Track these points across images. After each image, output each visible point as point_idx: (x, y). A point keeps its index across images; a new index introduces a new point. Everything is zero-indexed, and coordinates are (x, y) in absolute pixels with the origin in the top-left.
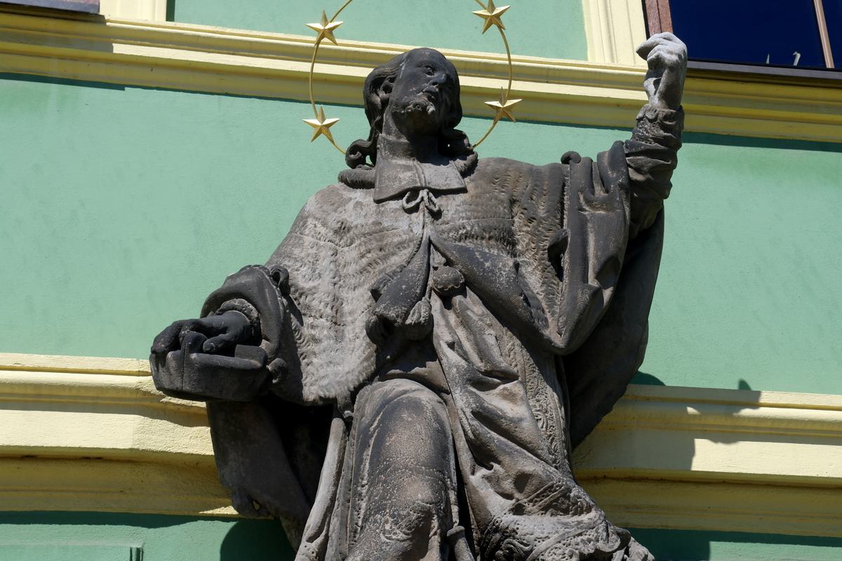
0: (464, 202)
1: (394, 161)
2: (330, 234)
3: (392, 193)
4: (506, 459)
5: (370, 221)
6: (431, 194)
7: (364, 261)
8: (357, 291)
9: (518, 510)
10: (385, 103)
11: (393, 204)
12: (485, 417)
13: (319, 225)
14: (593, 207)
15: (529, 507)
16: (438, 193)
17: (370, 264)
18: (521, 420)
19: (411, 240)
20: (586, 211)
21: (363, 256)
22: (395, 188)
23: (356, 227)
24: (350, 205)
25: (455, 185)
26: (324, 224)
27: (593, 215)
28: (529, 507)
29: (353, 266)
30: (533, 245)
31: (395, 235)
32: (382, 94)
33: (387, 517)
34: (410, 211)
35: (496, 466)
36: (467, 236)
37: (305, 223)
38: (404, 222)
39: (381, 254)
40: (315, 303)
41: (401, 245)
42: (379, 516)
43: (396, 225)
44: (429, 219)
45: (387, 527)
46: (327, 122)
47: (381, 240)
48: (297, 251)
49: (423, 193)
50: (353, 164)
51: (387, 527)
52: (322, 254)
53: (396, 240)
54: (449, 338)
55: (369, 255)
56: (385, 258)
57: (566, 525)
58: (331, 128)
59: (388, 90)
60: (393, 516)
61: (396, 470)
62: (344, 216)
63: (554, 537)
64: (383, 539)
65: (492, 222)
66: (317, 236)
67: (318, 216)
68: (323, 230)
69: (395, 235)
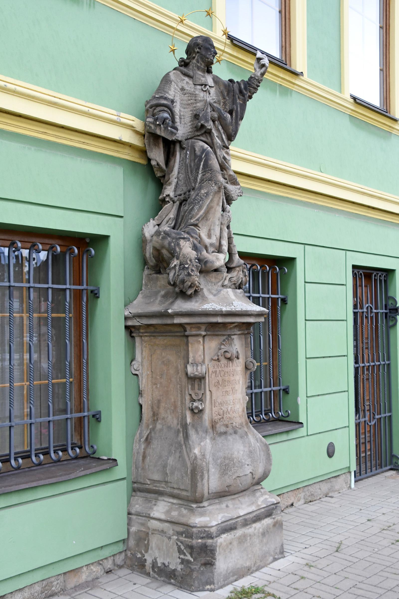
1: (198, 72)
2: (179, 89)
3: (199, 84)
4: (228, 170)
5: (192, 90)
7: (189, 102)
8: (186, 110)
9: (227, 183)
10: (198, 52)
11: (199, 87)
12: (224, 158)
13: (175, 85)
14: (240, 100)
16: (209, 86)
17: (191, 104)
19: (204, 100)
21: (189, 100)
22: (200, 82)
23: (187, 90)
24: (185, 82)
26: (177, 86)
27: (239, 102)
28: (229, 183)
29: (185, 102)
30: (224, 106)
31: (199, 97)
32: (198, 50)
33: (213, 183)
34: (204, 91)
35: (225, 172)
37: (171, 83)
38: (202, 94)
39: (195, 102)
40: (176, 111)
41: (201, 101)
42: (210, 182)
43: (200, 94)
45: (213, 185)
46: (175, 48)
47: (196, 97)
48: (170, 92)
49: (208, 87)
50: (181, 66)
51: (213, 185)
52: (176, 95)
53: (200, 99)
54: (216, 135)
55: (191, 101)
56: (196, 103)
57: (236, 188)
58: (175, 51)
59: (200, 48)
60: (215, 183)
61: (214, 171)
62: (183, 85)
63: (234, 191)
64: (212, 188)
66: (175, 89)
67: (176, 82)
68: (177, 88)
69: (199, 97)
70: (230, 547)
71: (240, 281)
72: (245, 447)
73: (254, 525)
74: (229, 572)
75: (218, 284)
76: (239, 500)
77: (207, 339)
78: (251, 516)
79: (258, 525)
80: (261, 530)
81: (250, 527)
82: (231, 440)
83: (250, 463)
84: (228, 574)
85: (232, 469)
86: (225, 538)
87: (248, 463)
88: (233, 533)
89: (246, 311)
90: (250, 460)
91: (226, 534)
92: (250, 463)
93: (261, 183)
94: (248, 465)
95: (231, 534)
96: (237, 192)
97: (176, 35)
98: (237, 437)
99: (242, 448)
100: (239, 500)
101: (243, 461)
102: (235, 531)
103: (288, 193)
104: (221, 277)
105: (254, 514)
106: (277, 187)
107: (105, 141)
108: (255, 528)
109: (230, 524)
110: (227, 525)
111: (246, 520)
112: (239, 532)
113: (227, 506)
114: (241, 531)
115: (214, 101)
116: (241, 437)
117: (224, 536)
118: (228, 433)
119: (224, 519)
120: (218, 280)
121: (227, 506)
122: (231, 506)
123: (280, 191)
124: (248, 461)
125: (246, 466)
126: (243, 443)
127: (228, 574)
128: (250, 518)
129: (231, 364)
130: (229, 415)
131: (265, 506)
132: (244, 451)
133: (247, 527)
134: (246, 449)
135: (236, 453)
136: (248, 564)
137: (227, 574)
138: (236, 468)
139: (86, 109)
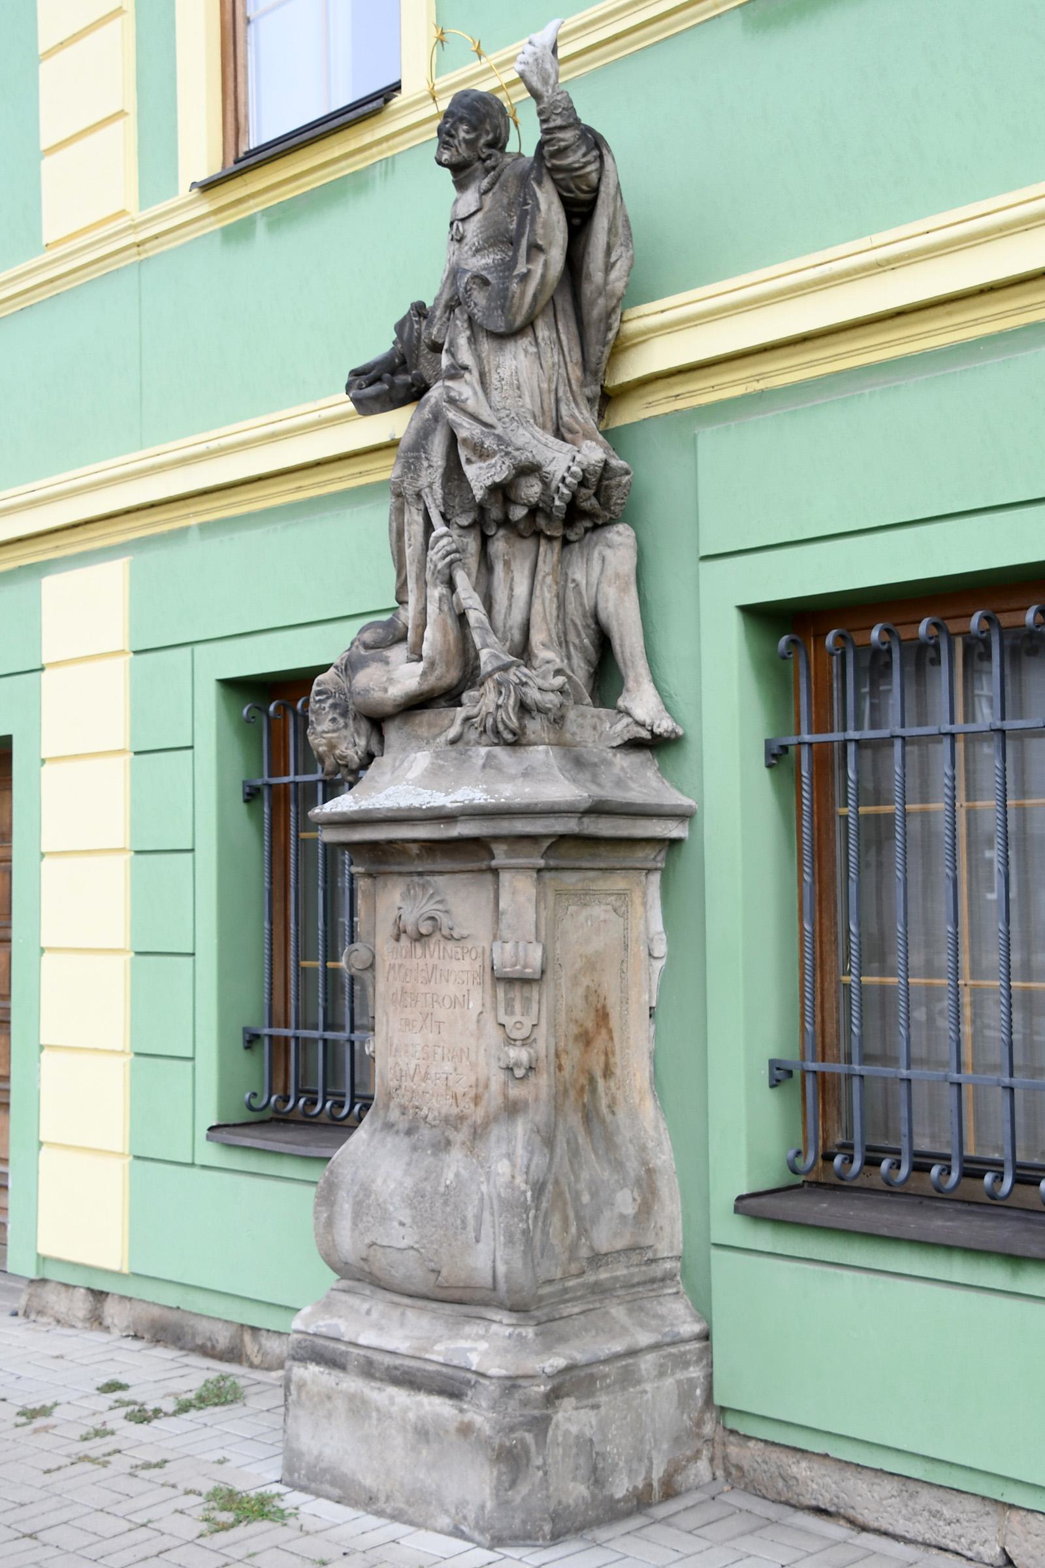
0: (479, 221)
6: (460, 224)
15: (474, 459)
16: (463, 220)
18: (467, 399)
20: (528, 204)
25: (473, 209)
28: (474, 459)
36: (477, 251)
44: (457, 246)
57: (480, 468)
65: (490, 232)
70: (328, 1405)
71: (490, 721)
72: (406, 1173)
73: (392, 1390)
74: (323, 1465)
75: (438, 740)
76: (403, 1314)
77: (380, 881)
78: (388, 1360)
79: (401, 1397)
80: (411, 1416)
81: (379, 1389)
82: (389, 1145)
83: (408, 1221)
84: (320, 1469)
85: (364, 1219)
86: (314, 1374)
87: (402, 1219)
88: (337, 1374)
89: (410, 809)
90: (408, 1212)
91: (322, 1369)
92: (408, 1221)
93: (854, 339)
94: (402, 1224)
95: (329, 1374)
96: (481, 479)
97: (516, 95)
98: (404, 1143)
99: (398, 1173)
100: (403, 1314)
101: (391, 1209)
102: (341, 1375)
103: (1022, 310)
104: (446, 722)
105: (398, 1362)
106: (950, 314)
107: (347, 462)
108: (392, 1399)
109: (334, 1350)
110: (326, 1347)
111: (370, 1362)
112: (352, 1383)
113: (368, 1312)
114: (354, 1381)
115: (474, 248)
116: (415, 1149)
117: (313, 1368)
118: (395, 1128)
119: (324, 1330)
120: (436, 730)
121: (368, 1312)
122: (375, 1315)
123: (976, 322)
124: (405, 1215)
125: (395, 1224)
126: (409, 1164)
127: (320, 1469)
128: (383, 1364)
129: (419, 951)
130: (412, 1084)
131: (441, 1360)
132: (401, 1184)
133: (373, 1384)
134: (409, 1182)
135: (379, 1181)
136: (369, 1481)
137: (318, 1469)
138: (371, 1219)
139: (313, 417)
